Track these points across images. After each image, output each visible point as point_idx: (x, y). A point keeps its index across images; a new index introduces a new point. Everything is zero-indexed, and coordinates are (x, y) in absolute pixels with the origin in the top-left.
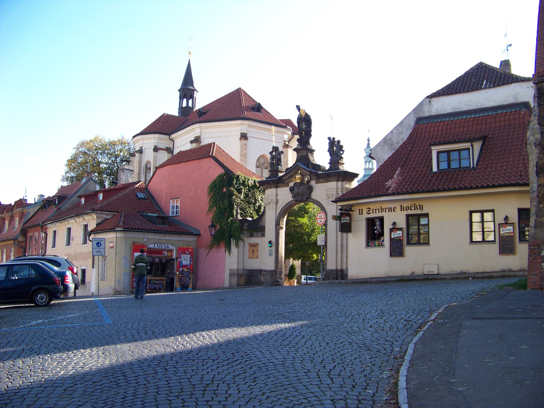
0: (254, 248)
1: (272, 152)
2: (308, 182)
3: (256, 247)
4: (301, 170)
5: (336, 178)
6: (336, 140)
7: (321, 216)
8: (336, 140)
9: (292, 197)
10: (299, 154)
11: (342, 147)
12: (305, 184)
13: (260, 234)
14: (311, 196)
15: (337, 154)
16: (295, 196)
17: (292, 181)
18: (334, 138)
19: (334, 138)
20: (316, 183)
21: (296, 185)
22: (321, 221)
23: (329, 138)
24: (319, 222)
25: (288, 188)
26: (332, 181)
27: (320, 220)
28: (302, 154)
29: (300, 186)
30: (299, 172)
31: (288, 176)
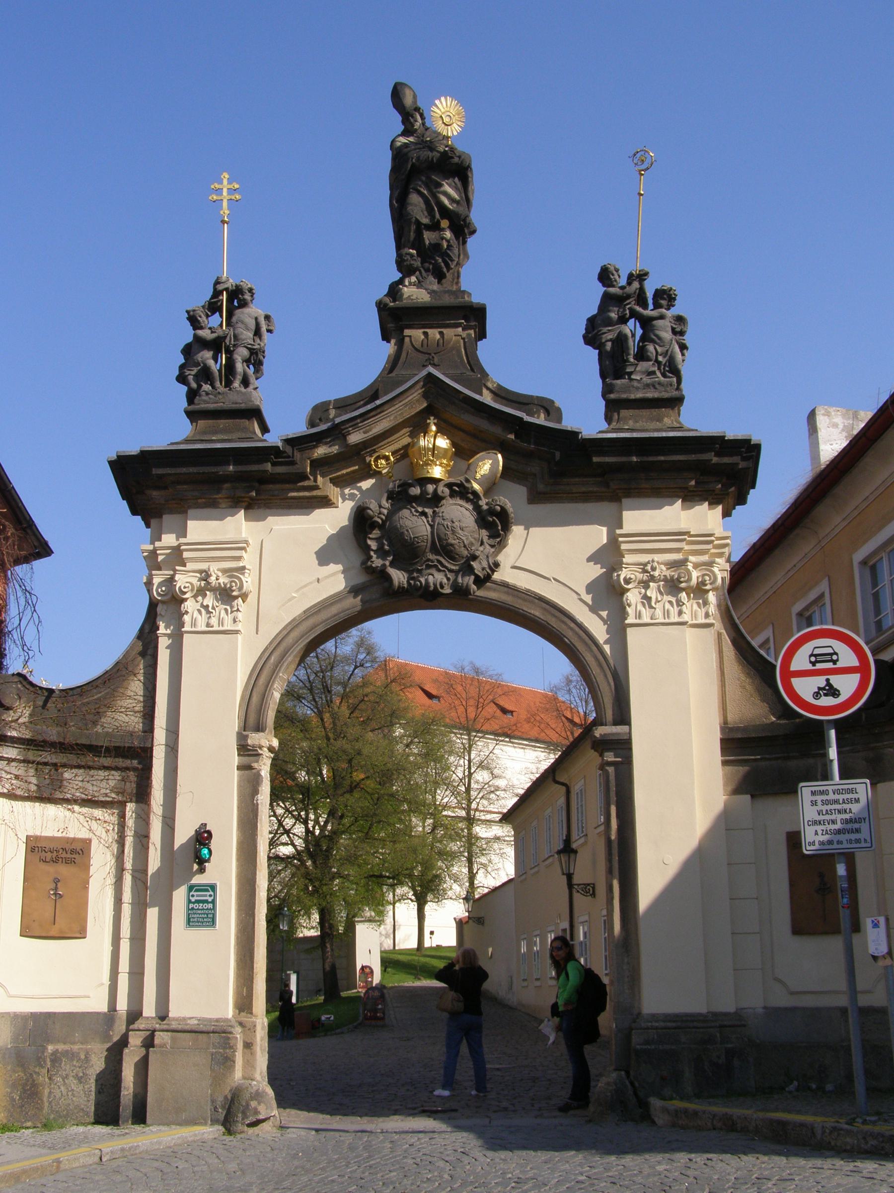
0: (63, 870)
3: (73, 862)
7: (831, 657)
10: (407, 332)
12: (475, 493)
22: (832, 692)
24: (810, 699)
27: (821, 681)
28: (434, 334)
31: (355, 438)
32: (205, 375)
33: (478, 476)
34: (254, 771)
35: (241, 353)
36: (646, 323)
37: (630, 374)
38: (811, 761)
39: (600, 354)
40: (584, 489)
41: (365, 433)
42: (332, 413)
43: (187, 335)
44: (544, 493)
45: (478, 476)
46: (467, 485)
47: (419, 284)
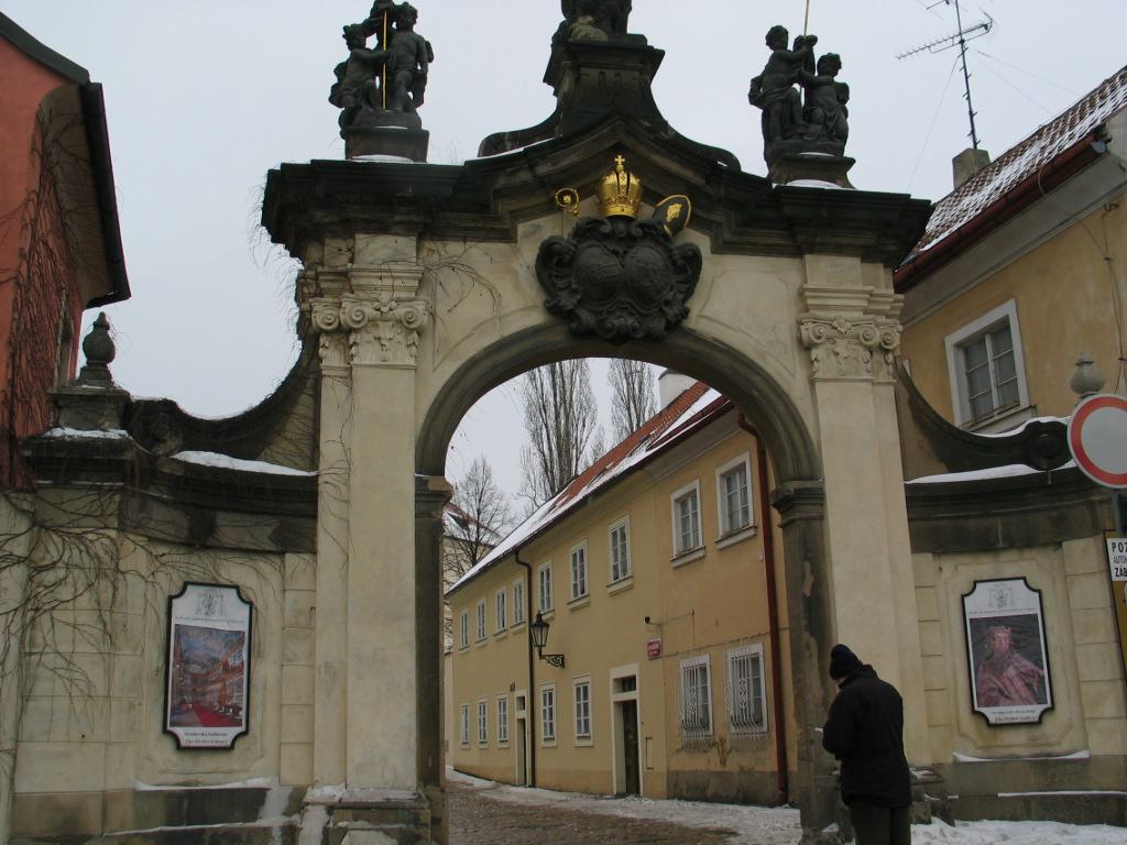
1: (370, 27)
2: (678, 225)
4: (643, 150)
5: (868, 239)
6: (819, 52)
8: (819, 52)
9: (553, 309)
11: (843, 91)
12: (665, 235)
13: (263, 533)
14: (685, 313)
15: (831, 124)
16: (579, 302)
17: (552, 207)
18: (807, 42)
19: (807, 42)
20: (721, 248)
21: (606, 228)
23: (776, 37)
25: (528, 253)
26: (839, 250)
28: (610, 74)
29: (631, 240)
30: (620, 160)
32: (368, 95)
33: (669, 219)
34: (433, 520)
35: (403, 75)
36: (811, 87)
37: (802, 135)
38: (991, 521)
39: (765, 117)
40: (770, 241)
41: (553, 165)
42: (509, 144)
43: (344, 54)
44: (730, 243)
45: (669, 219)
46: (659, 227)
47: (595, 24)
